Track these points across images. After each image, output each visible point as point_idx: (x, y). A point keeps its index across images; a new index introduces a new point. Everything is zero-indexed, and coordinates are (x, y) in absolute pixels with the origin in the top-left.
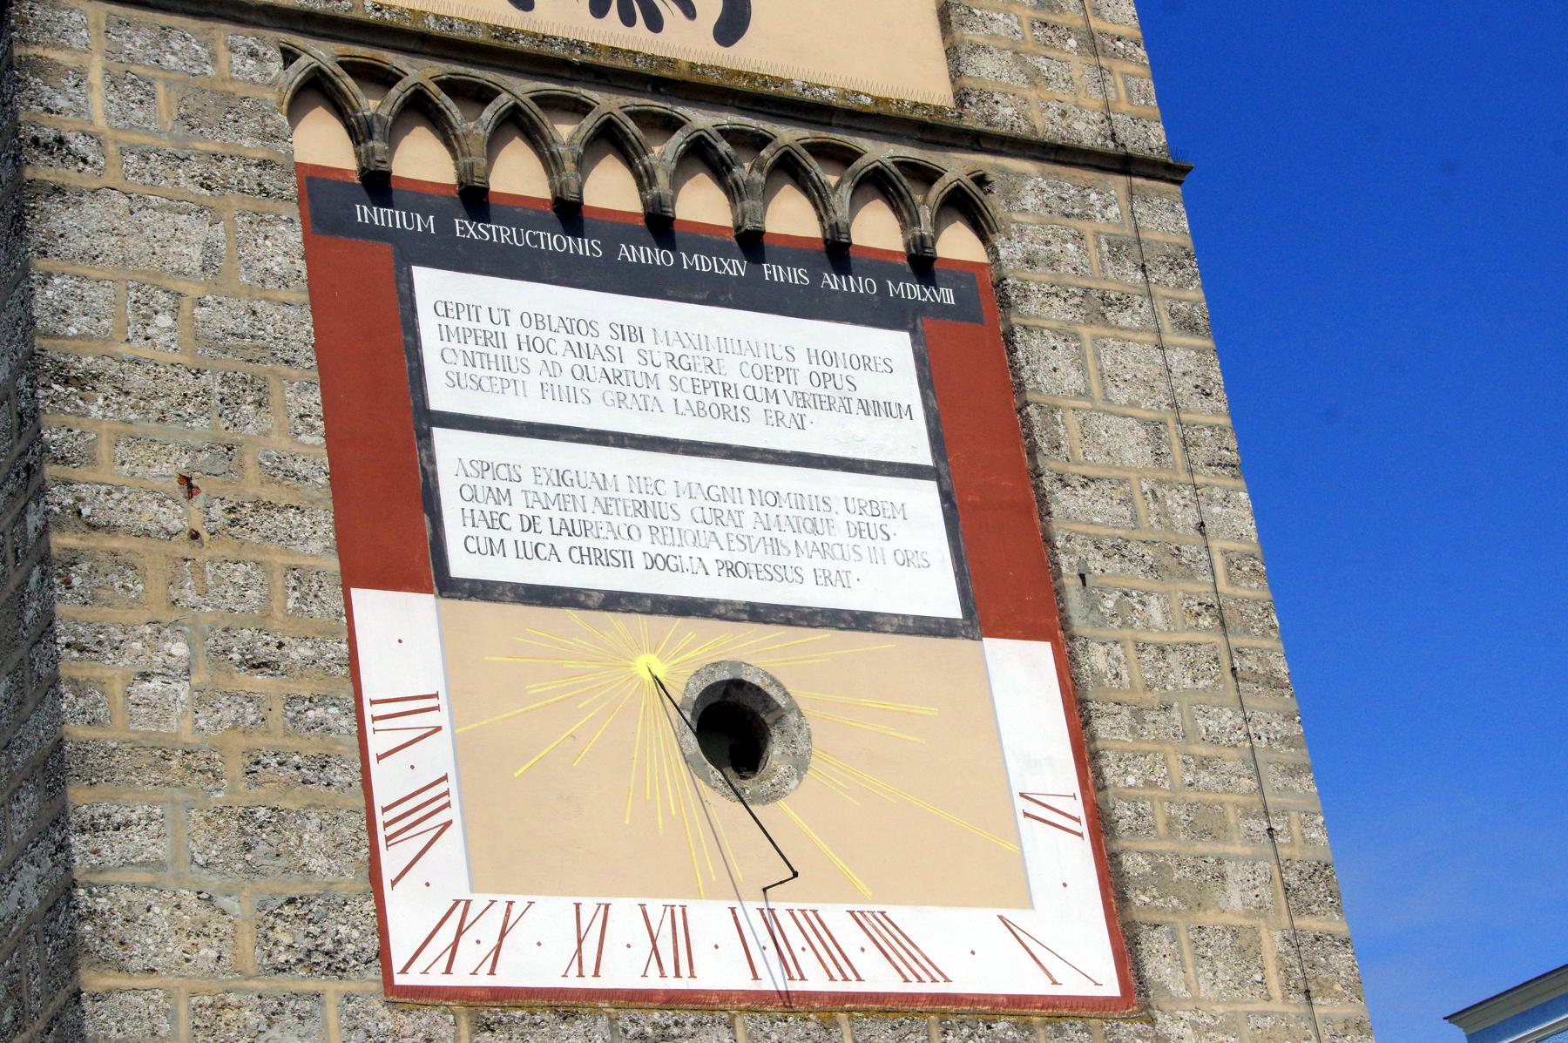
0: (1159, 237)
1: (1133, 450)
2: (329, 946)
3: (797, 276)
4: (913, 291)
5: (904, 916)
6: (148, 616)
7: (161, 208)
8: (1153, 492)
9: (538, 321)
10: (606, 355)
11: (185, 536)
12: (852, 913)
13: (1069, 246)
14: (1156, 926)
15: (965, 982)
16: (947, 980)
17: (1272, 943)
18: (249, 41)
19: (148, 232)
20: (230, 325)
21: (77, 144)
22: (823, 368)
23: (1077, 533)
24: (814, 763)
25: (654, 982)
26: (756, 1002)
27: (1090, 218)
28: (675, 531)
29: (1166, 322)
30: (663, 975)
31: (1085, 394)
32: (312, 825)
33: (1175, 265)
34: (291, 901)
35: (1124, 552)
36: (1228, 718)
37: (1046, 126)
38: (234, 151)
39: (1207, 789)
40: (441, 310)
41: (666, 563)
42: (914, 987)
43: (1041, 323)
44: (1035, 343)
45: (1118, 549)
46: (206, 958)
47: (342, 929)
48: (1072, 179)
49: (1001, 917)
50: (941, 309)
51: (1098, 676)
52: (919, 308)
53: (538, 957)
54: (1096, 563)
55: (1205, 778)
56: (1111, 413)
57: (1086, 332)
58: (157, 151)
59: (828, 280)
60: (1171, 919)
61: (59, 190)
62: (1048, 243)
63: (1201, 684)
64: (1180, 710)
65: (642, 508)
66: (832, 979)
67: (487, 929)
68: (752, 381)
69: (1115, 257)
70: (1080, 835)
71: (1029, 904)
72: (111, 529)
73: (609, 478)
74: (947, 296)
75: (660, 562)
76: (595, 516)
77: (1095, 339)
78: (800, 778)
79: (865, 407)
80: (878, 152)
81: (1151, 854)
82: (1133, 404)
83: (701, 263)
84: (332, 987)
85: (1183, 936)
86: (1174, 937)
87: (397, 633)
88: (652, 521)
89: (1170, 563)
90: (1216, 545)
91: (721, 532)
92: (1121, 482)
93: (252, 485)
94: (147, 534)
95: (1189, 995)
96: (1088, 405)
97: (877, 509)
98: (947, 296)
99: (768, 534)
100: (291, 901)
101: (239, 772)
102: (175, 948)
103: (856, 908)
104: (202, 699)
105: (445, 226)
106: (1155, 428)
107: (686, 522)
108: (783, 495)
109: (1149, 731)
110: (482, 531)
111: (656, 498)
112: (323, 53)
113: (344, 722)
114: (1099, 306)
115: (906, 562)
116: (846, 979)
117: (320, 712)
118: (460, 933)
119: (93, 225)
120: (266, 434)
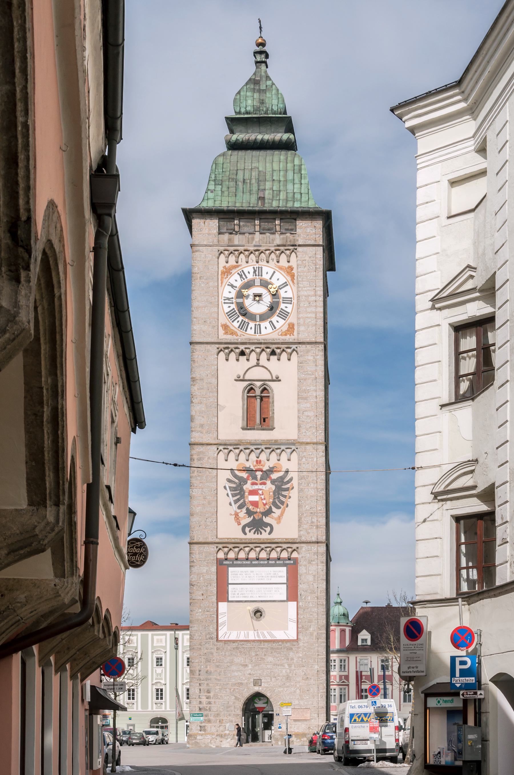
1: (311, 578)
3: (273, 562)
5: (273, 632)
9: (242, 572)
15: (278, 638)
17: (315, 634)
21: (195, 561)
25: (244, 639)
26: (254, 641)
29: (319, 562)
33: (322, 555)
36: (316, 609)
37: (309, 539)
45: (306, 591)
48: (309, 546)
50: (291, 564)
52: (288, 564)
53: (233, 637)
54: (303, 593)
57: (308, 565)
59: (278, 562)
65: (251, 591)
67: (228, 635)
71: (287, 630)
74: (292, 562)
76: (245, 592)
80: (285, 546)
83: (262, 562)
84: (211, 641)
87: (223, 606)
89: (313, 592)
90: (319, 589)
97: (278, 588)
98: (292, 562)
102: (198, 637)
104: (202, 615)
105: (233, 562)
106: (314, 576)
112: (220, 546)
114: (310, 562)
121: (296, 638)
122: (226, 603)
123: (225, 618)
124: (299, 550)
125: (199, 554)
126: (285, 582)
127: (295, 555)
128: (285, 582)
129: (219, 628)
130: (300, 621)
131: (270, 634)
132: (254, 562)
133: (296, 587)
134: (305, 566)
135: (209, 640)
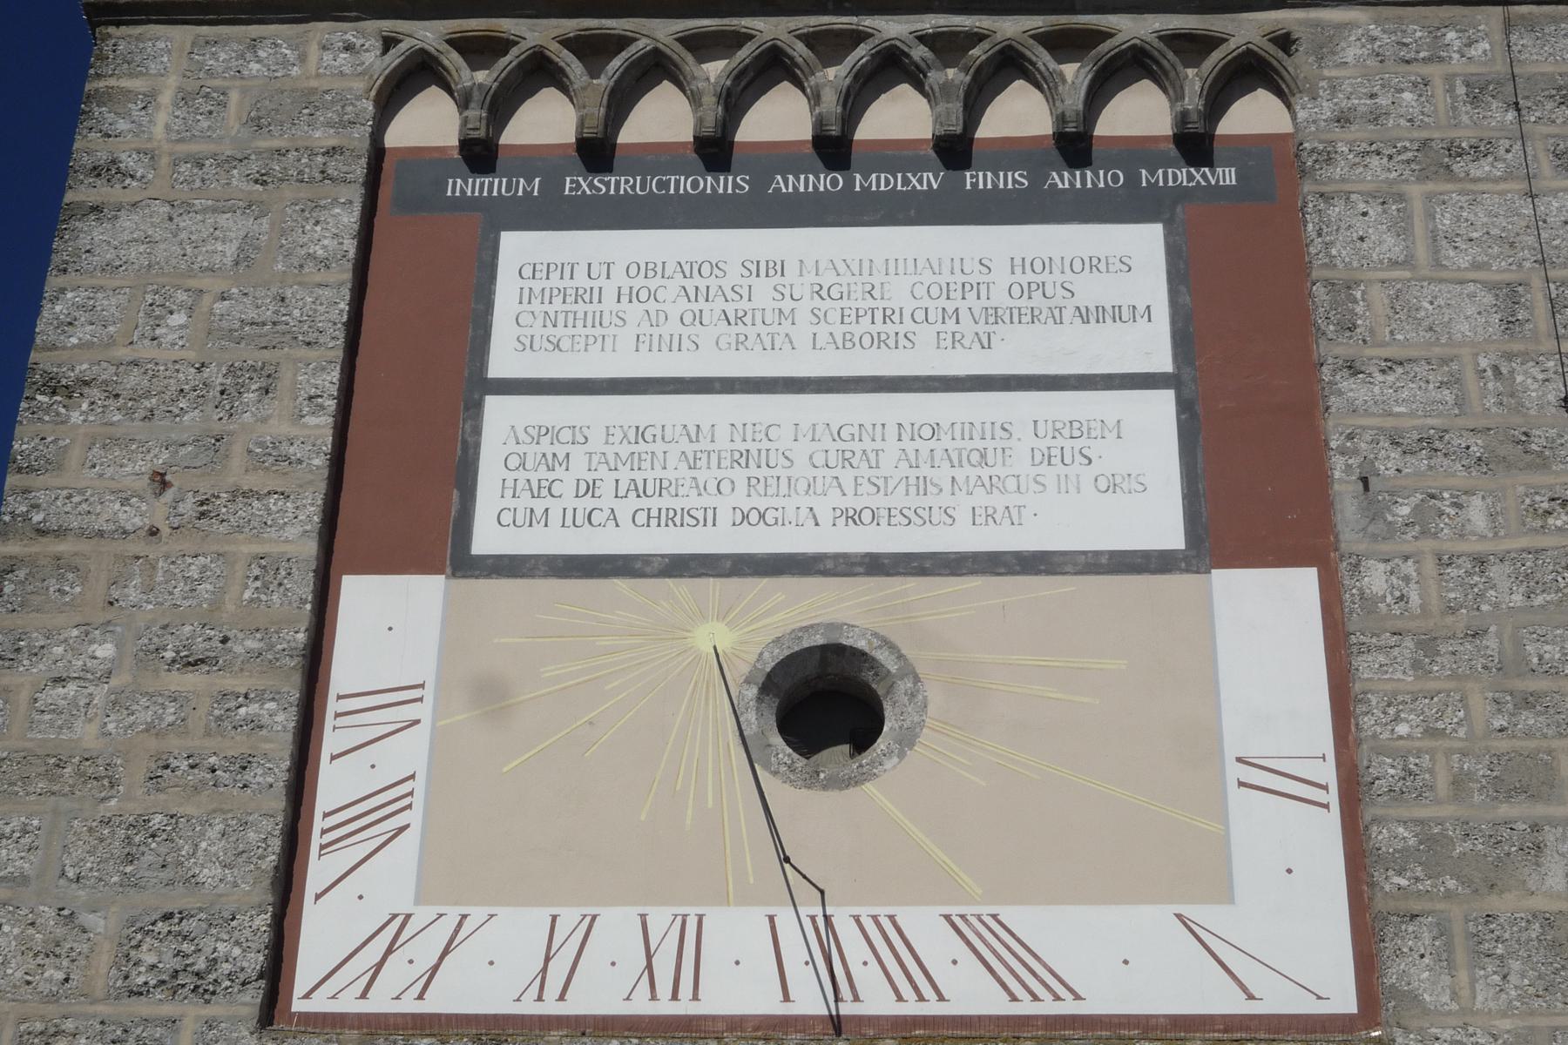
0: (1549, 69)
1: (1470, 318)
2: (201, 965)
3: (1013, 179)
4: (1182, 175)
5: (1022, 918)
6: (78, 619)
7: (204, 210)
8: (1496, 369)
9: (648, 269)
10: (730, 294)
11: (143, 533)
12: (947, 917)
13: (1407, 96)
14: (1414, 917)
16: (1077, 997)
18: (348, 36)
19: (184, 235)
20: (252, 314)
21: (128, 162)
22: (1030, 277)
23: (1364, 428)
24: (926, 736)
25: (641, 1006)
27: (1441, 60)
28: (784, 481)
30: (654, 997)
31: (1408, 262)
32: (213, 833)
34: (167, 917)
35: (1437, 444)
38: (300, 143)
39: (1528, 734)
40: (527, 272)
41: (762, 516)
42: (1026, 1008)
43: (1347, 187)
44: (1335, 211)
45: (1428, 443)
46: (50, 980)
47: (221, 947)
49: (1179, 916)
51: (1369, 602)
52: (1182, 194)
54: (1389, 462)
55: (1528, 719)
56: (1441, 281)
57: (1415, 191)
58: (214, 156)
60: (1440, 906)
61: (96, 209)
62: (1372, 96)
63: (1539, 600)
64: (1499, 635)
66: (900, 998)
68: (927, 302)
69: (1474, 100)
70: (1326, 806)
71: (1223, 892)
72: (60, 533)
73: (705, 429)
74: (1227, 176)
75: (754, 517)
76: (677, 471)
77: (1429, 197)
78: (902, 755)
79: (1084, 316)
81: (1421, 822)
82: (1476, 266)
83: (879, 182)
84: (192, 1012)
85: (1457, 928)
86: (1442, 931)
88: (753, 471)
91: (847, 477)
92: (1445, 361)
93: (237, 473)
94: (101, 534)
95: (1454, 1007)
96: (1407, 274)
97: (1077, 429)
98: (1227, 176)
99: (913, 473)
100: (167, 917)
101: (141, 776)
103: (953, 910)
106: (1510, 295)
107: (802, 469)
108: (945, 425)
109: (1442, 665)
110: (525, 501)
111: (765, 444)
113: (280, 718)
114: (1440, 159)
115: (1113, 487)
116: (921, 998)
117: (254, 708)
118: (390, 951)
119: (126, 236)
120: (264, 420)
121: (1345, 1002)
122: (438, 581)
123: (408, 754)
124: (1300, 64)
125: (184, 98)
126: (1163, 362)
127: (1253, 115)
128: (1163, 362)
129: (318, 870)
130: (1387, 771)
131: (988, 944)
132: (786, 184)
133: (1301, 414)
134: (1387, 196)
135: (158, 1006)
